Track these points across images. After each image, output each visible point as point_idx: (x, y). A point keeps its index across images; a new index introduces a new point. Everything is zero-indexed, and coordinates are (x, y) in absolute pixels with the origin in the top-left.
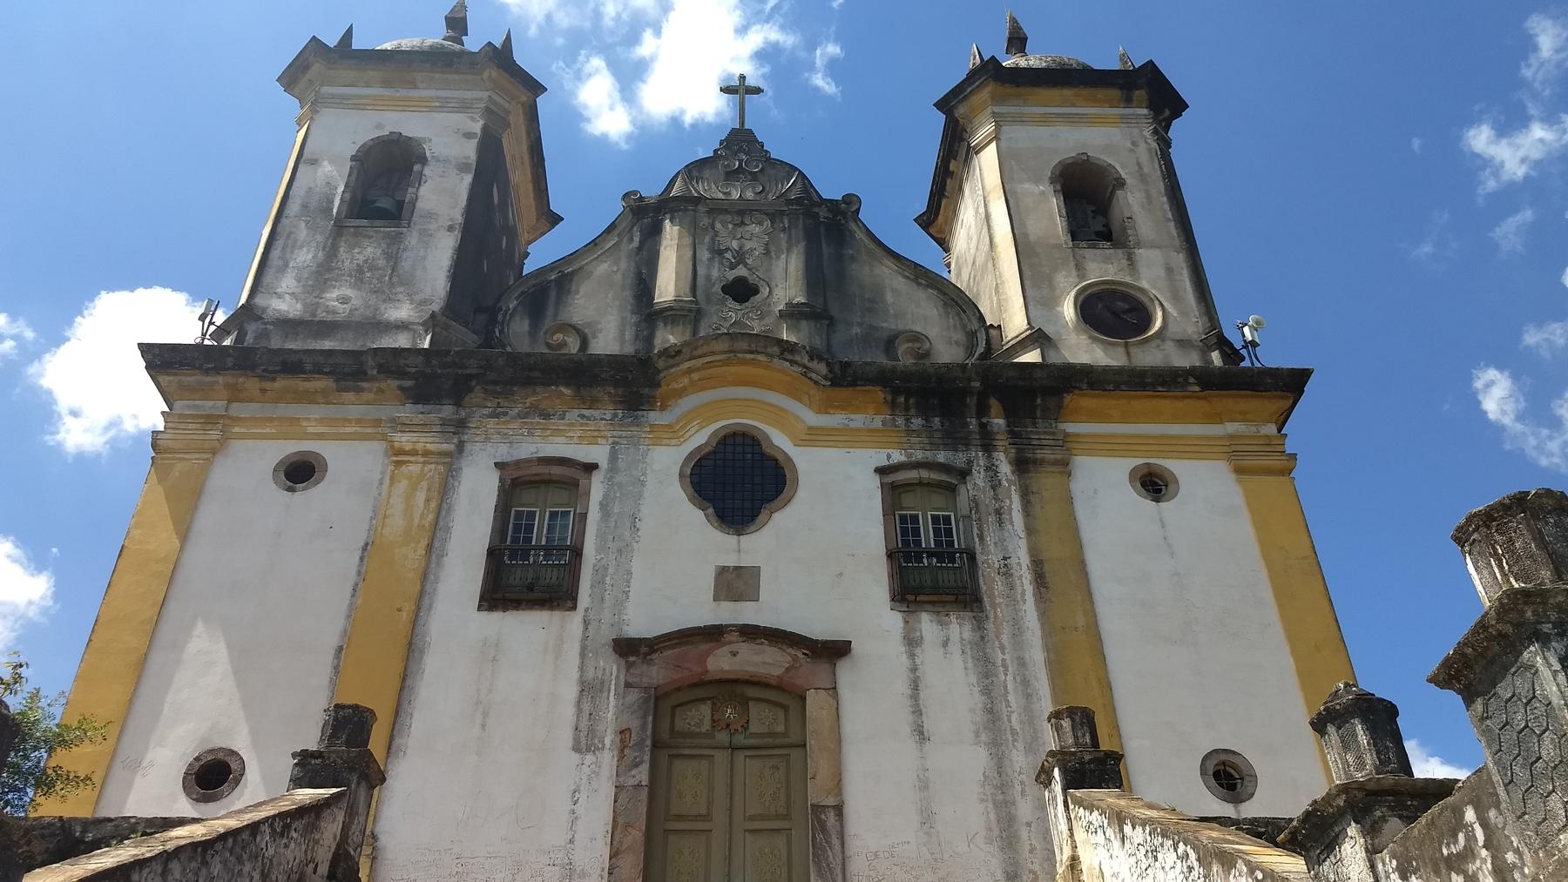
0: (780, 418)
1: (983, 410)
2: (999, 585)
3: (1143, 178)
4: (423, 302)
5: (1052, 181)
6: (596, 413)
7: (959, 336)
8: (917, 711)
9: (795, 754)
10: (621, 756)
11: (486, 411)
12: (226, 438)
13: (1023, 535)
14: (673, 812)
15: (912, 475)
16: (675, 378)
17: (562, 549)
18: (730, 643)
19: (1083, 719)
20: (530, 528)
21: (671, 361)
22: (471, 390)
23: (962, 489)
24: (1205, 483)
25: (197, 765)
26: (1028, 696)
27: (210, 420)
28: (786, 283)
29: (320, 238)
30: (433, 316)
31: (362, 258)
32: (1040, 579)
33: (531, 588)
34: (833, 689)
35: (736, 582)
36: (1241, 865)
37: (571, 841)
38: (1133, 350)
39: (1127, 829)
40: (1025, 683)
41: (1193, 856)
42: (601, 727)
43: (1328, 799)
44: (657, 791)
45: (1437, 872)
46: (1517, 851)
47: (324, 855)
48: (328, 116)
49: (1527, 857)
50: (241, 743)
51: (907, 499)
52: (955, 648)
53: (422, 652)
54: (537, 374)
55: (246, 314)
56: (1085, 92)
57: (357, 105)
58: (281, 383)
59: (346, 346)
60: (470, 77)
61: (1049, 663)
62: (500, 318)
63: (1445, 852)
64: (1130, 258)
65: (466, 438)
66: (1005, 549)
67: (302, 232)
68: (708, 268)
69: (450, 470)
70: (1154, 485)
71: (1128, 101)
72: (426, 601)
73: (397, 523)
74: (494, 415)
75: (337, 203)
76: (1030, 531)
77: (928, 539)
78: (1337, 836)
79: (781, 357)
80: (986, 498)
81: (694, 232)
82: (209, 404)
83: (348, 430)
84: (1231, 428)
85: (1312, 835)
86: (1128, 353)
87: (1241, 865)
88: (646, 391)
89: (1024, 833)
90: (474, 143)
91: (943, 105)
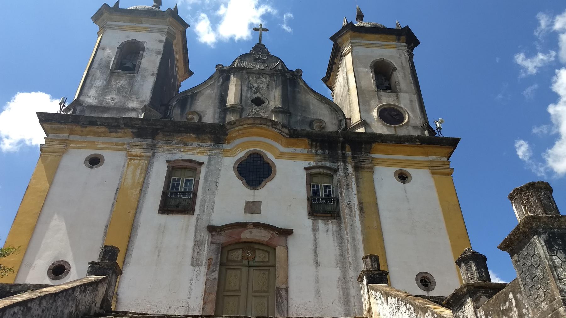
0: (271, 148)
1: (343, 148)
2: (347, 211)
3: (403, 68)
4: (141, 101)
5: (371, 68)
6: (204, 144)
7: (336, 122)
8: (316, 255)
9: (271, 269)
10: (209, 268)
11: (163, 142)
12: (67, 148)
13: (356, 193)
14: (227, 288)
15: (317, 171)
16: (233, 132)
17: (189, 193)
18: (250, 228)
19: (375, 259)
20: (178, 185)
21: (232, 126)
22: (158, 134)
23: (335, 176)
24: (421, 177)
25: (53, 266)
26: (355, 251)
27: (62, 141)
28: (274, 100)
29: (105, 76)
30: (145, 106)
31: (120, 84)
32: (361, 209)
33: (177, 206)
34: (286, 246)
35: (252, 207)
36: (429, 312)
37: (189, 298)
38: (397, 129)
39: (389, 298)
40: (355, 246)
41: (412, 308)
42: (201, 258)
43: (461, 289)
44: (221, 282)
45: (498, 316)
46: (527, 309)
47: (99, 300)
48: (109, 32)
49: (530, 311)
50: (69, 259)
51: (315, 179)
52: (330, 233)
53: (137, 228)
54: (183, 129)
55: (77, 103)
56: (384, 36)
57: (121, 29)
58: (89, 129)
59: (113, 116)
60: (162, 20)
61: (364, 240)
62: (170, 108)
63: (502, 308)
64: (397, 96)
65: (155, 151)
66: (349, 198)
67: (98, 74)
68: (247, 93)
69: (150, 163)
70: (403, 177)
71: (399, 40)
72: (139, 210)
73: (129, 181)
74: (166, 143)
75: (111, 64)
76: (359, 192)
77: (322, 193)
78: (464, 302)
79: (272, 126)
80: (343, 180)
81: (242, 80)
82: (62, 135)
83: (112, 147)
84: (431, 158)
85: (455, 302)
86: (395, 130)
87: (429, 312)
88: (222, 136)
89: (352, 299)
90: (162, 44)
91: (332, 38)
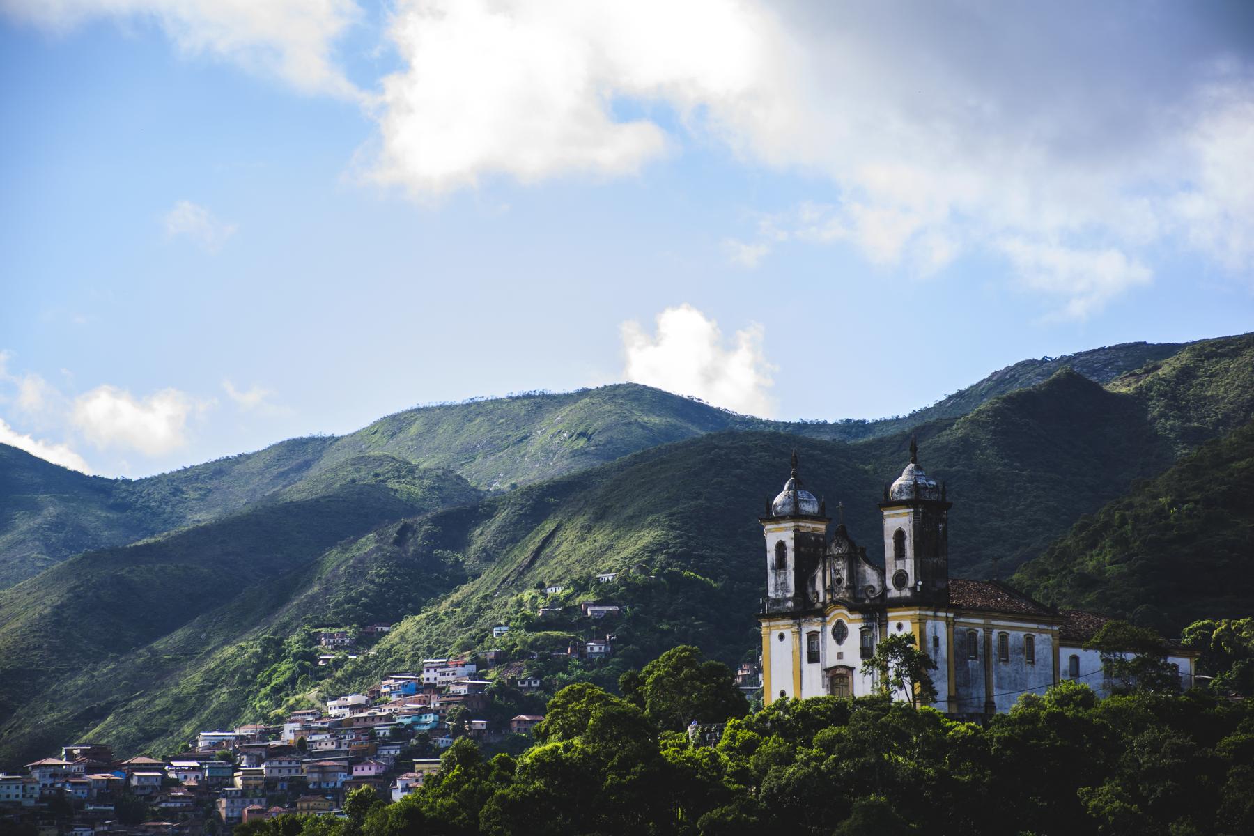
35: (840, 656)
84: (911, 613)
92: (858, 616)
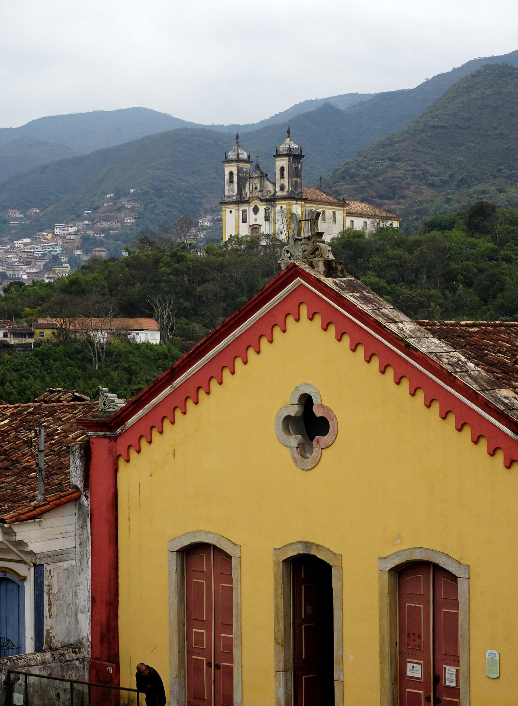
35: (256, 220)
84: (287, 202)
92: (264, 203)
